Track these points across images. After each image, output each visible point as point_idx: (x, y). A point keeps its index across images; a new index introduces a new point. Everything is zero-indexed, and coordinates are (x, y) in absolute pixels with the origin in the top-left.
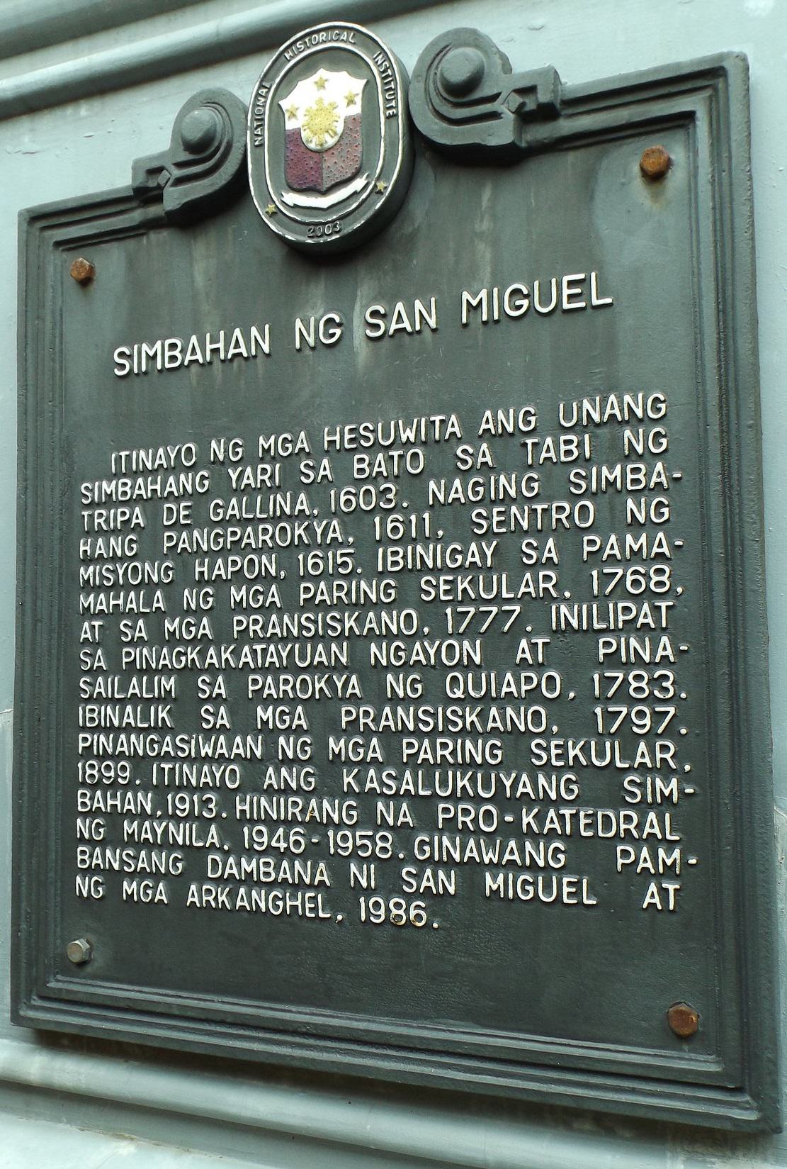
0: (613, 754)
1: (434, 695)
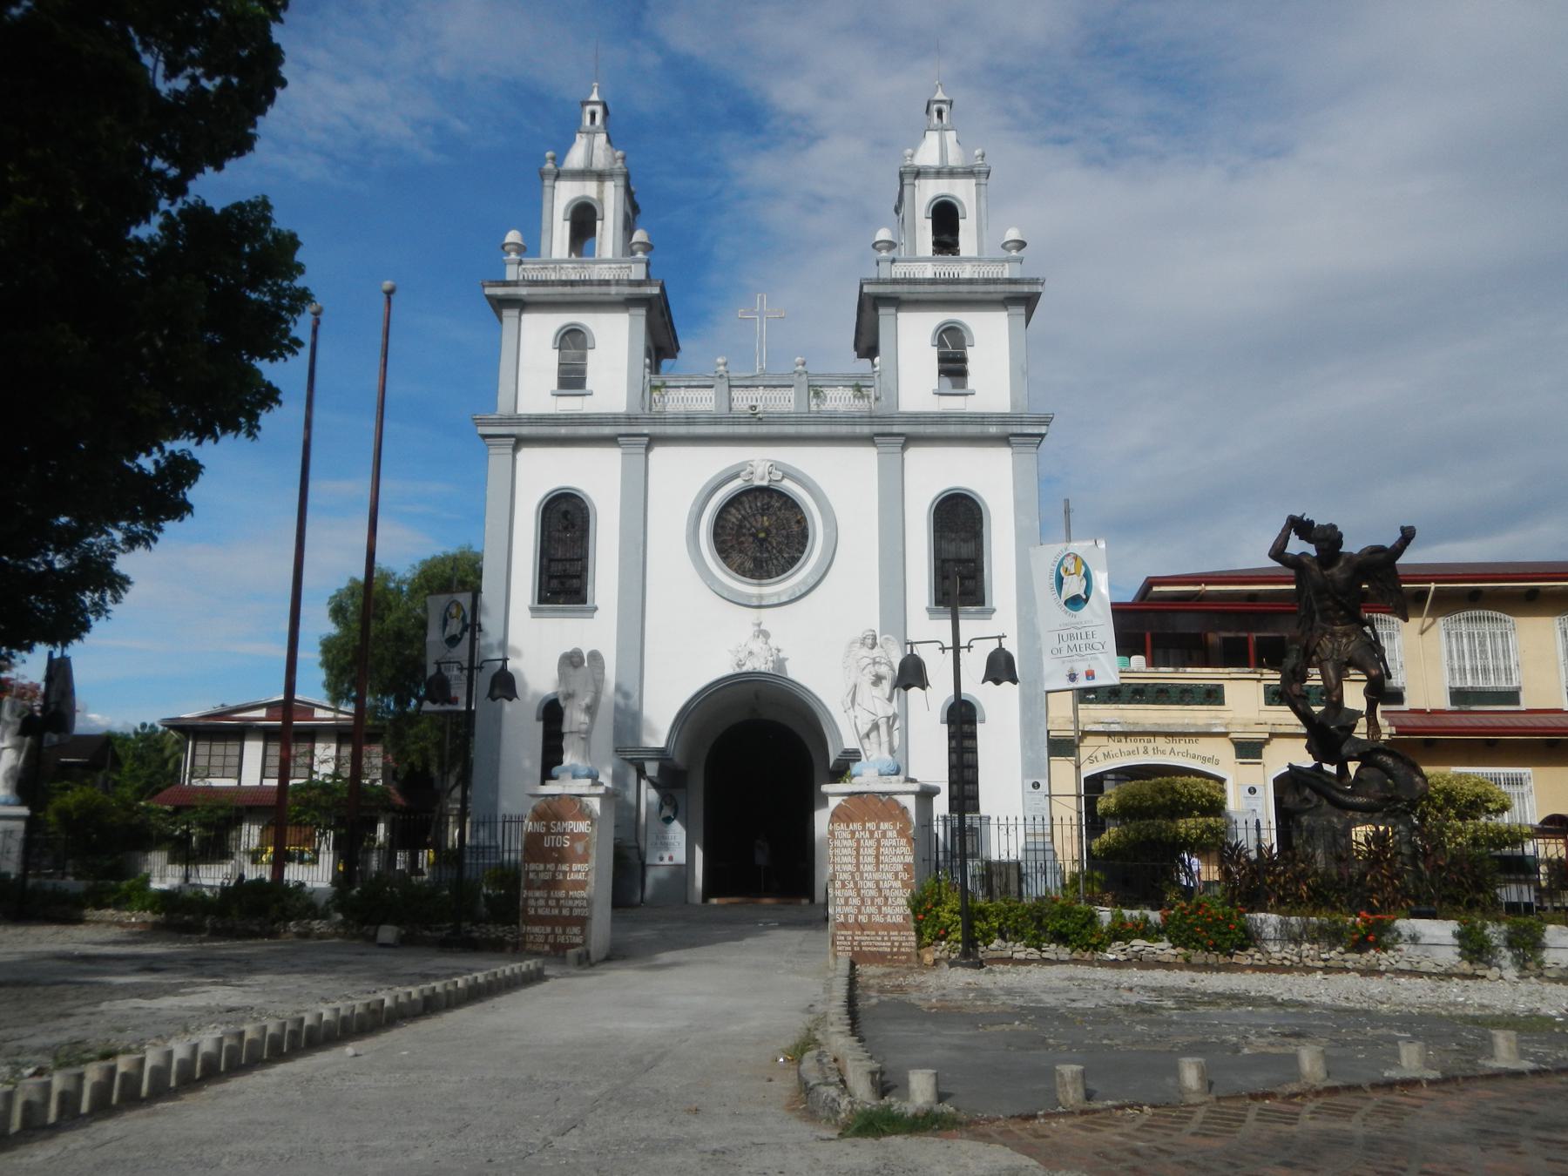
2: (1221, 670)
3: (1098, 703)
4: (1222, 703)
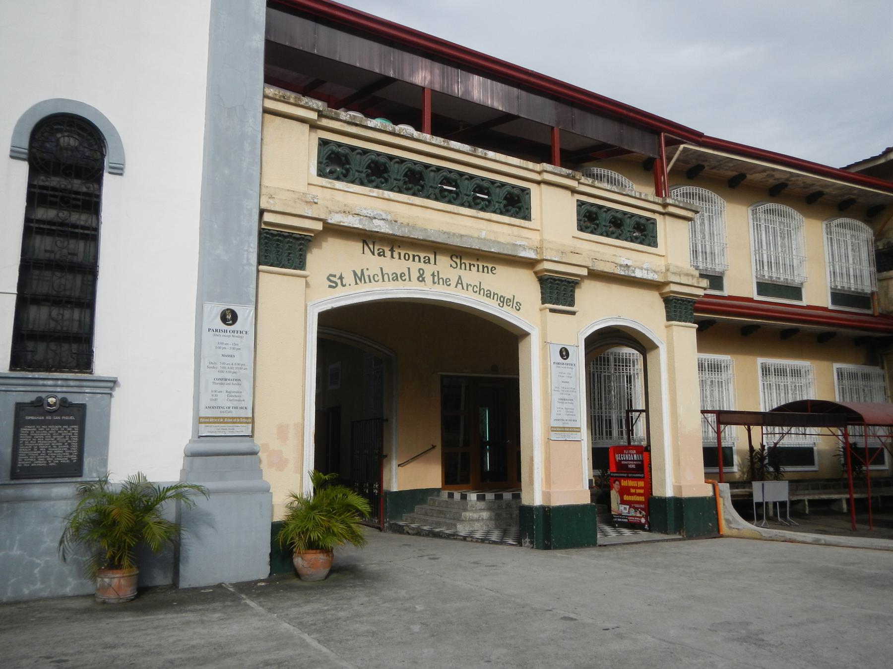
0: (72, 451)
1: (57, 446)
2: (531, 165)
3: (353, 182)
4: (527, 217)
